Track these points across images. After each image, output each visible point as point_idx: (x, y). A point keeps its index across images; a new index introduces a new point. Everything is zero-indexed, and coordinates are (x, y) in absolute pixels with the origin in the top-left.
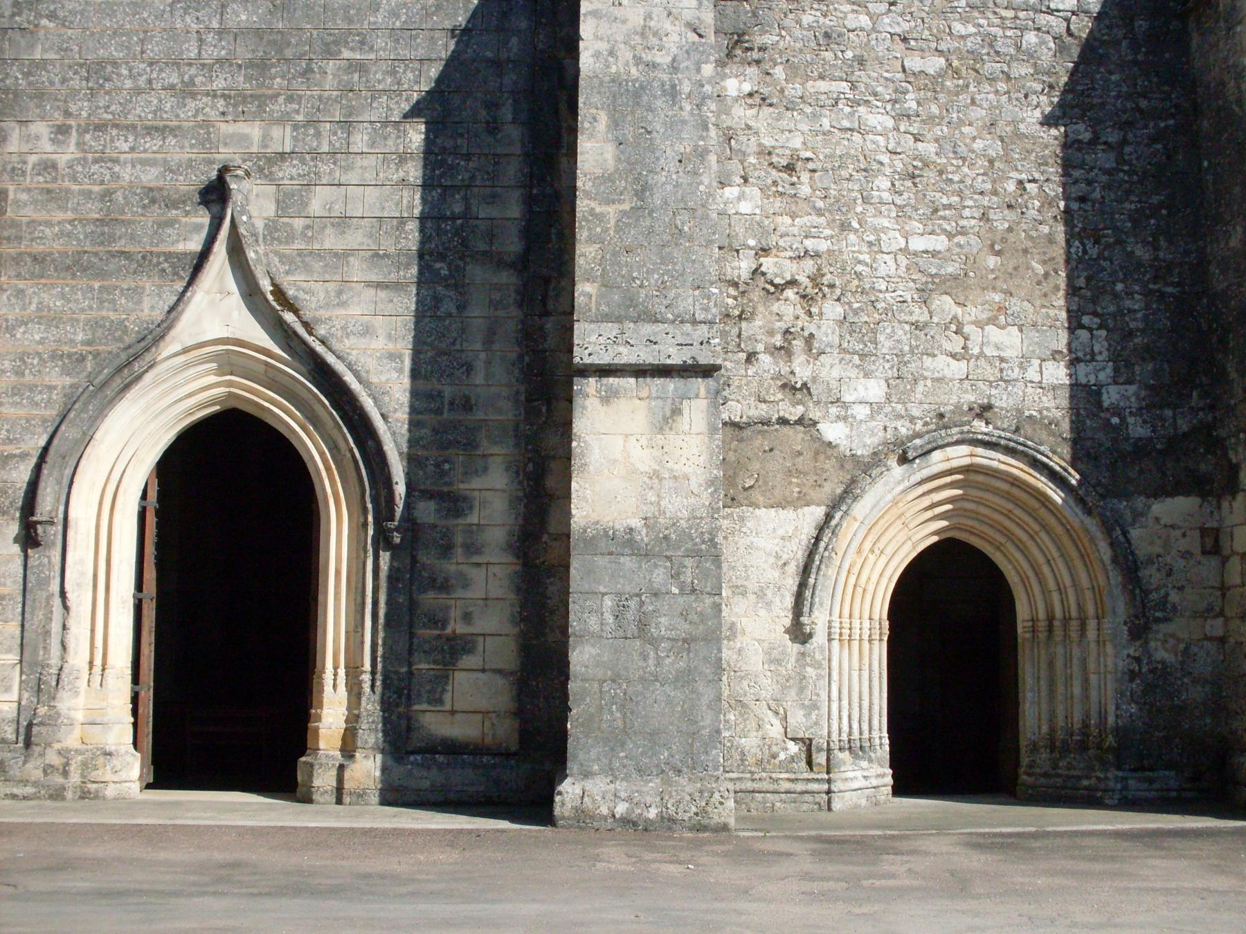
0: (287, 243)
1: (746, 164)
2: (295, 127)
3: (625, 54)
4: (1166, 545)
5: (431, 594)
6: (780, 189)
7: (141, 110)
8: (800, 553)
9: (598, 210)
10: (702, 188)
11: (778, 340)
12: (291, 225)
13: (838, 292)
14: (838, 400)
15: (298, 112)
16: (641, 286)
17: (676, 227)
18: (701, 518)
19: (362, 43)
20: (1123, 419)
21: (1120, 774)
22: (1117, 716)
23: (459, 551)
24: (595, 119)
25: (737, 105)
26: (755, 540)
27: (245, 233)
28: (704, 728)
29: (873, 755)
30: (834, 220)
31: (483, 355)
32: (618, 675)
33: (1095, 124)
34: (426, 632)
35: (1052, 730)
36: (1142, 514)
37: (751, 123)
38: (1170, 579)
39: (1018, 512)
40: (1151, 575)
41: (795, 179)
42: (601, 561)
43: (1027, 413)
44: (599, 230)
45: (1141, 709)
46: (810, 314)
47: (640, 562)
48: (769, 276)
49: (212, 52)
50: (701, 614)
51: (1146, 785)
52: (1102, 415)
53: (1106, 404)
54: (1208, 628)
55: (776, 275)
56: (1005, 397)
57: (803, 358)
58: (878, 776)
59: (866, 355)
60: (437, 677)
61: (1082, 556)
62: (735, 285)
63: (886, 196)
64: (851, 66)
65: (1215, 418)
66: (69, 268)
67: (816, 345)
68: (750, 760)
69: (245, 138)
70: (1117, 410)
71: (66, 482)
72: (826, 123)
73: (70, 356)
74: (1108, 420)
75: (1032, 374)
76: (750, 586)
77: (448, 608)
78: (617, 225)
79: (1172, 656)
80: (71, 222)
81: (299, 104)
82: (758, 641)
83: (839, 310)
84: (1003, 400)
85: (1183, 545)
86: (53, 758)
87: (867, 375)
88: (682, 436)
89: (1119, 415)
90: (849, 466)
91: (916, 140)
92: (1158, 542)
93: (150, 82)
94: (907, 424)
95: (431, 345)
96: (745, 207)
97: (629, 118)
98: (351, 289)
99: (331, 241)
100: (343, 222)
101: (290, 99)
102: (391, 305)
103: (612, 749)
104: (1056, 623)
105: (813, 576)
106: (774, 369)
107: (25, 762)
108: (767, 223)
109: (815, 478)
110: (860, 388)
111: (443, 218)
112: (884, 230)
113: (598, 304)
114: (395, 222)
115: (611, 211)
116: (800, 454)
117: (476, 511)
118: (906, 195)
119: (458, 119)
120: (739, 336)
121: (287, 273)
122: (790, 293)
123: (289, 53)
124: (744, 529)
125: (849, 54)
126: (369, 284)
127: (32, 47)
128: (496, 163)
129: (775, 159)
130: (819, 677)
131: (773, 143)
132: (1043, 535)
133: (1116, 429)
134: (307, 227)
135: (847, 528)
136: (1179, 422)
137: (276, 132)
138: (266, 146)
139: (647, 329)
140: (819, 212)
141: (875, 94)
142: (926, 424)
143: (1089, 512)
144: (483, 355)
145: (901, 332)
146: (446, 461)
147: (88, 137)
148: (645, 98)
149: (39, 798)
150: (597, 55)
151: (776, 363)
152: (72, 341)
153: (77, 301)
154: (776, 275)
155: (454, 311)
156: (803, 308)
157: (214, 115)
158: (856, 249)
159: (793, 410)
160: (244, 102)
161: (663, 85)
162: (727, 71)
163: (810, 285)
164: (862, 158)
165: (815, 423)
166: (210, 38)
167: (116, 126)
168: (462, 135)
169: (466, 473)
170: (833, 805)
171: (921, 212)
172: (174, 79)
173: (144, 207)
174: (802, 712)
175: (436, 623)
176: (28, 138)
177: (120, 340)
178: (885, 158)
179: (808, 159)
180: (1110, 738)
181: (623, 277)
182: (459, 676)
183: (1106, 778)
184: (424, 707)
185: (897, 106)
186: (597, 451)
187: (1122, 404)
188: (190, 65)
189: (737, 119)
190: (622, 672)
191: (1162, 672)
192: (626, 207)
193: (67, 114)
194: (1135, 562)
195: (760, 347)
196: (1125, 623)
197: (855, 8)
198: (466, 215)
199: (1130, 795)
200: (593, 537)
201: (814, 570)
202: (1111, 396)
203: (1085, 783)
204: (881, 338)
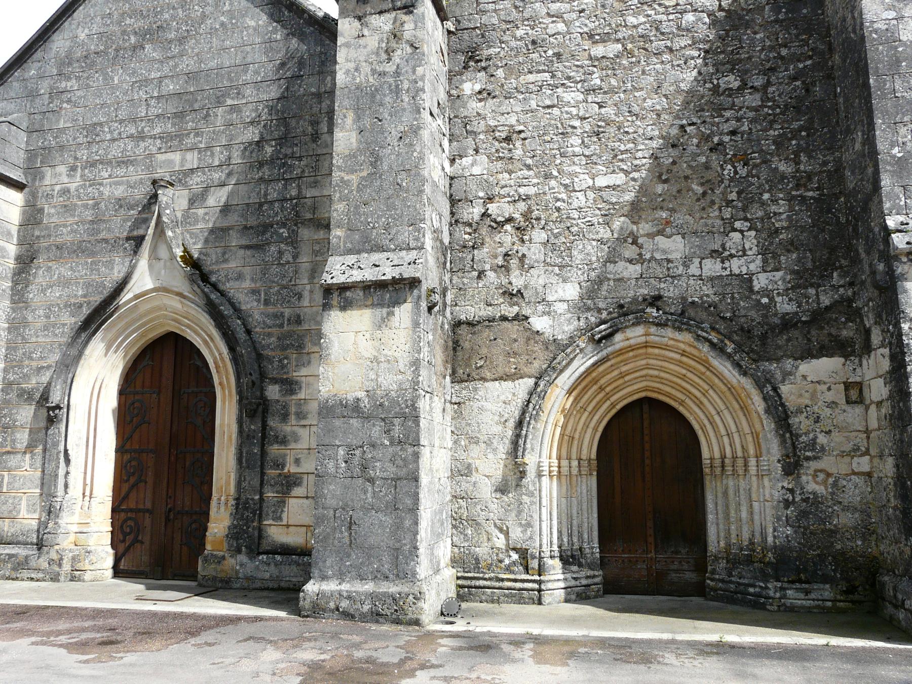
0: (194, 225)
1: (477, 141)
2: (200, 153)
3: (366, 69)
4: (813, 396)
5: (276, 447)
6: (501, 155)
7: (115, 151)
8: (517, 412)
9: (346, 178)
10: (415, 154)
11: (500, 261)
12: (196, 214)
13: (543, 222)
14: (544, 300)
15: (201, 142)
16: (373, 228)
17: (398, 184)
18: (406, 389)
19: (238, 94)
20: (772, 299)
21: (779, 584)
22: (775, 537)
23: (293, 417)
24: (345, 116)
25: (470, 101)
26: (485, 404)
27: (166, 220)
28: (405, 545)
29: (583, 561)
30: (539, 172)
31: (308, 287)
32: (347, 506)
33: (743, 76)
34: (272, 472)
35: (728, 545)
36: (790, 374)
37: (481, 112)
38: (818, 425)
39: (689, 375)
40: (800, 422)
41: (511, 146)
42: (338, 423)
43: (690, 300)
44: (346, 191)
45: (795, 532)
46: (523, 241)
47: (363, 423)
48: (493, 217)
49: (154, 111)
50: (404, 460)
51: (802, 596)
52: (754, 297)
53: (756, 289)
54: (854, 465)
55: (498, 215)
56: (672, 289)
57: (517, 272)
58: (587, 577)
59: (564, 267)
60: (278, 502)
61: (742, 408)
62: (470, 225)
63: (577, 150)
64: (552, 61)
65: (854, 293)
66: (75, 251)
67: (527, 262)
68: (482, 564)
69: (171, 162)
70: (766, 292)
71: (69, 381)
72: (533, 104)
73: (74, 305)
74: (759, 301)
75: (694, 269)
76: (482, 437)
77: (285, 455)
78: (358, 186)
79: (823, 488)
80: (77, 224)
81: (202, 137)
82: (487, 476)
83: (543, 236)
84: (670, 291)
85: (830, 396)
86: (54, 556)
87: (564, 281)
88: (394, 331)
89: (768, 296)
90: (552, 348)
91: (601, 107)
92: (807, 395)
93: (120, 134)
94: (596, 314)
95: (277, 283)
96: (476, 170)
97: (367, 112)
98: (230, 251)
101: (197, 135)
102: (253, 259)
103: (341, 559)
104: (727, 461)
105: (525, 429)
106: (497, 281)
107: (39, 557)
108: (491, 179)
109: (527, 357)
110: (560, 291)
111: (286, 200)
112: (576, 174)
113: (345, 243)
114: (257, 206)
115: (354, 178)
116: (516, 340)
117: (303, 390)
118: (592, 147)
119: (293, 135)
120: (472, 261)
121: (194, 244)
122: (508, 227)
123: (196, 106)
124: (477, 397)
125: (550, 53)
126: (241, 247)
127: (58, 121)
128: (318, 160)
129: (497, 134)
130: (532, 503)
131: (496, 123)
132: (711, 392)
133: (766, 307)
134: (206, 214)
135: (551, 393)
136: (822, 298)
137: (189, 156)
138: (183, 166)
139: (376, 257)
140: (529, 167)
141: (569, 78)
142: (610, 313)
143: (745, 374)
144: (308, 287)
145: (590, 247)
146: (286, 358)
147: (87, 171)
148: (378, 97)
149: (45, 580)
150: (347, 72)
151: (498, 277)
152: (76, 295)
153: (79, 271)
154: (498, 215)
155: (291, 259)
156: (517, 236)
157: (154, 150)
158: (556, 190)
159: (511, 309)
160: (171, 140)
161: (390, 86)
162: (464, 78)
163: (522, 220)
164: (559, 125)
165: (527, 318)
166: (153, 102)
167: (101, 163)
168: (297, 145)
169: (297, 366)
170: (543, 599)
171: (604, 158)
172: (133, 131)
173: (116, 210)
174: (520, 529)
175: (278, 466)
176: (55, 175)
177: (102, 293)
178: (577, 123)
179: (520, 132)
180: (770, 555)
181: (362, 222)
182: (292, 502)
183: (767, 588)
184: (270, 522)
185: (586, 84)
186: (336, 344)
187: (770, 287)
188: (142, 121)
189: (471, 110)
190: (350, 503)
191: (814, 501)
192: (365, 174)
193: (76, 158)
194: (785, 412)
195: (487, 267)
196: (779, 461)
197: (554, 19)
198: (299, 197)
199: (788, 602)
200: (333, 406)
201: (525, 424)
202: (761, 282)
203: (751, 590)
204: (575, 253)
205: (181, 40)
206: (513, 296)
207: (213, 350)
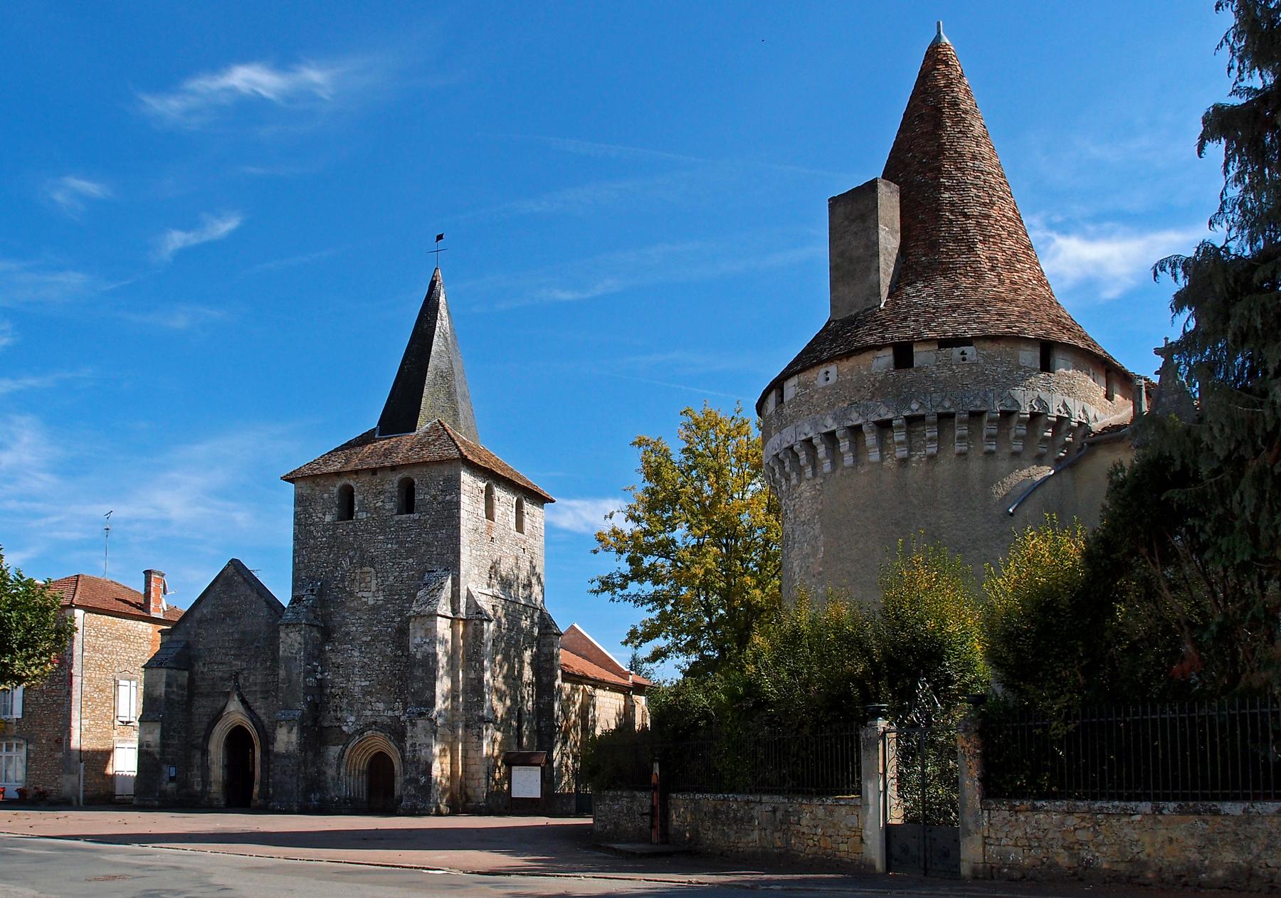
99: (254, 689)
100: (256, 684)
205: (239, 618)
206: (338, 719)
207: (253, 733)
